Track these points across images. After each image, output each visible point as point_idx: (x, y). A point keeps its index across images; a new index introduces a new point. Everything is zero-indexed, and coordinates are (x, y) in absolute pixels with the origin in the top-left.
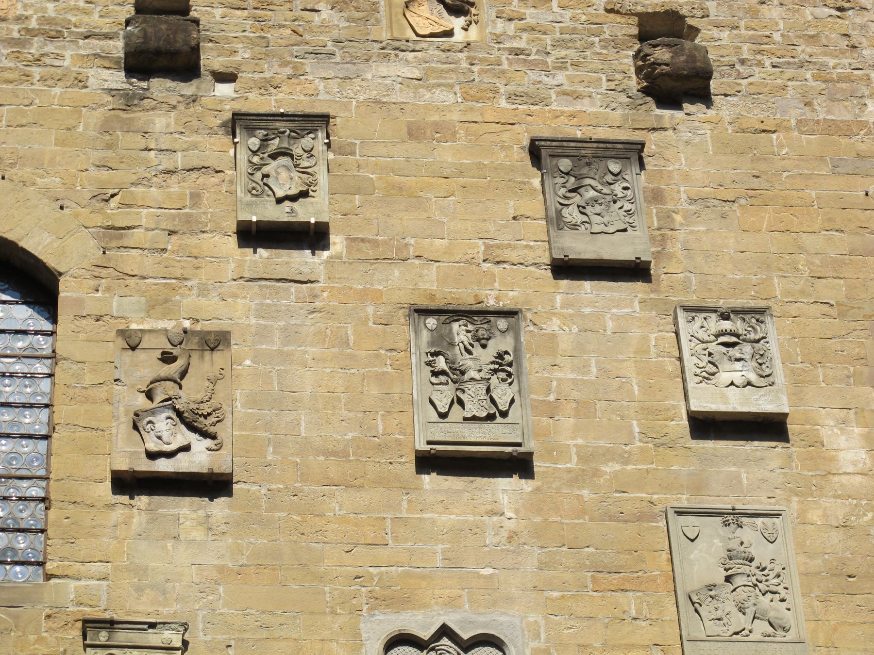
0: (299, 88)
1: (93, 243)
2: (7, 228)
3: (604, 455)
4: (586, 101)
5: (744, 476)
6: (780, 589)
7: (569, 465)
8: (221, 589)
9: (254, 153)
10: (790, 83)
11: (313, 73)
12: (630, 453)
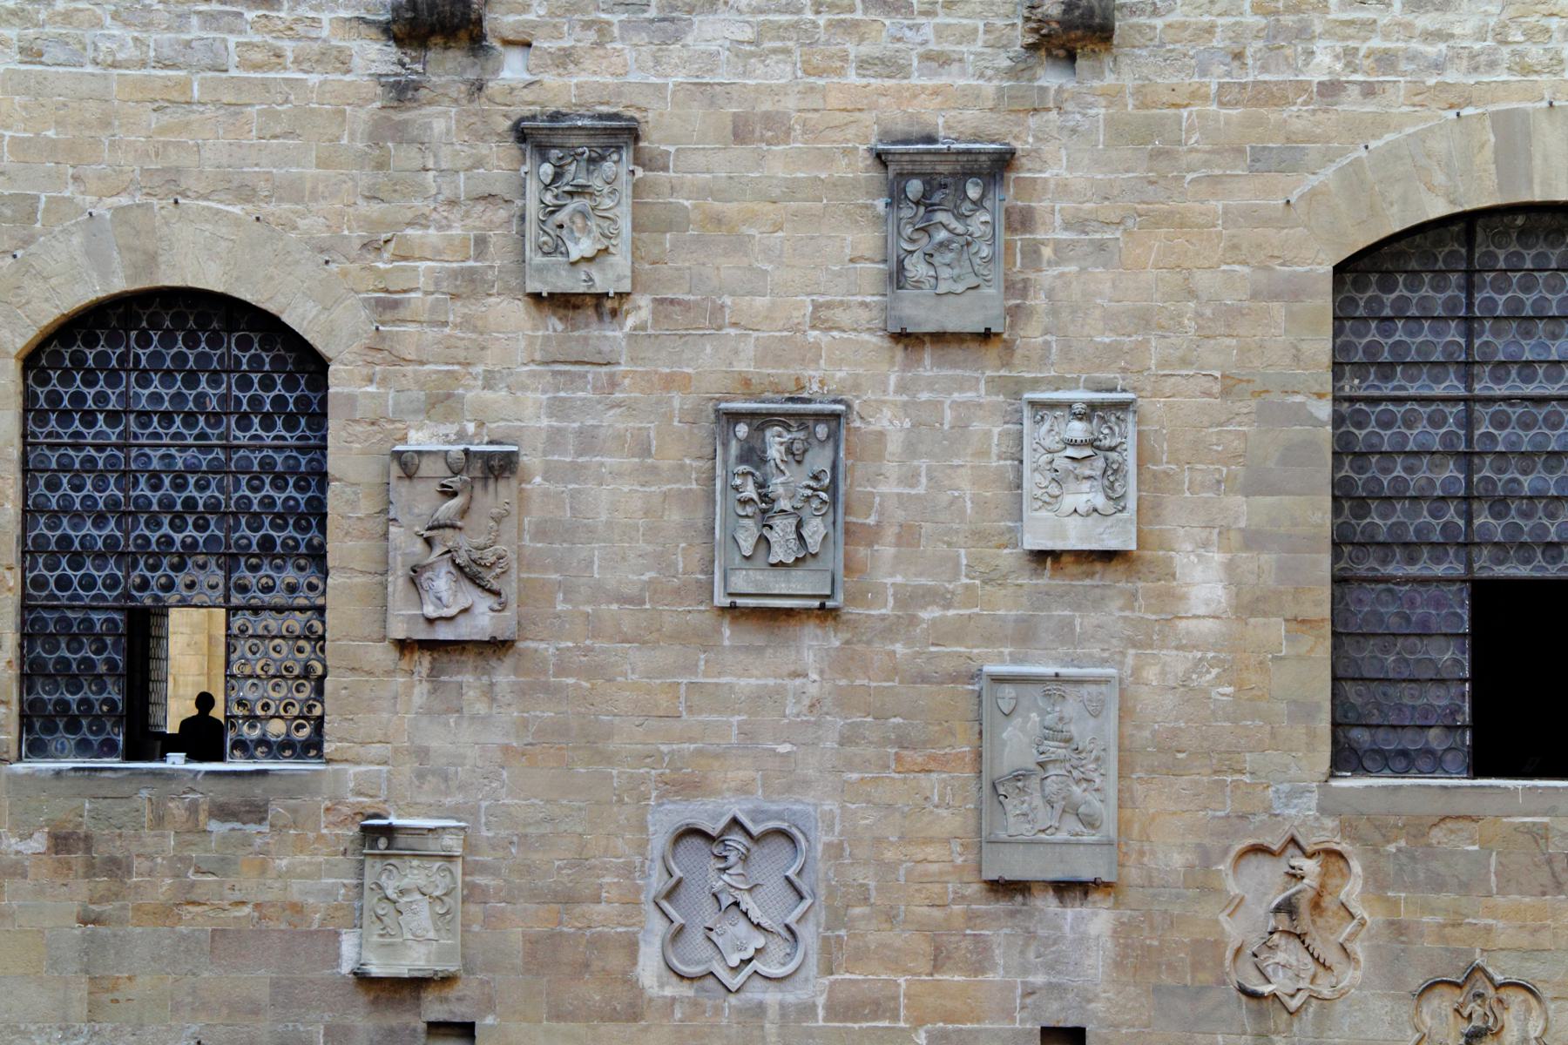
0: (605, 63)
1: (364, 314)
2: (266, 296)
3: (923, 596)
4: (955, 67)
5: (1078, 621)
6: (1095, 776)
7: (883, 611)
8: (505, 774)
9: (547, 187)
10: (1220, 21)
11: (622, 39)
12: (953, 593)
